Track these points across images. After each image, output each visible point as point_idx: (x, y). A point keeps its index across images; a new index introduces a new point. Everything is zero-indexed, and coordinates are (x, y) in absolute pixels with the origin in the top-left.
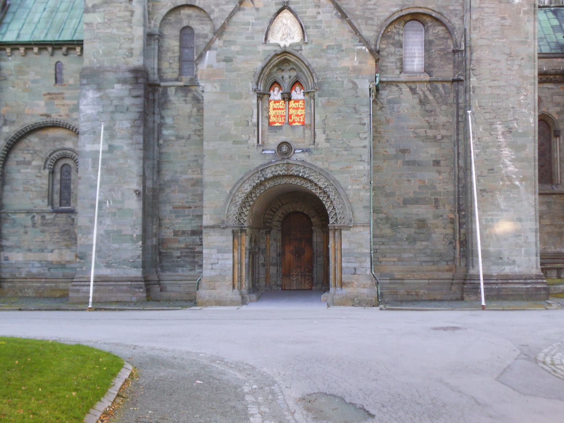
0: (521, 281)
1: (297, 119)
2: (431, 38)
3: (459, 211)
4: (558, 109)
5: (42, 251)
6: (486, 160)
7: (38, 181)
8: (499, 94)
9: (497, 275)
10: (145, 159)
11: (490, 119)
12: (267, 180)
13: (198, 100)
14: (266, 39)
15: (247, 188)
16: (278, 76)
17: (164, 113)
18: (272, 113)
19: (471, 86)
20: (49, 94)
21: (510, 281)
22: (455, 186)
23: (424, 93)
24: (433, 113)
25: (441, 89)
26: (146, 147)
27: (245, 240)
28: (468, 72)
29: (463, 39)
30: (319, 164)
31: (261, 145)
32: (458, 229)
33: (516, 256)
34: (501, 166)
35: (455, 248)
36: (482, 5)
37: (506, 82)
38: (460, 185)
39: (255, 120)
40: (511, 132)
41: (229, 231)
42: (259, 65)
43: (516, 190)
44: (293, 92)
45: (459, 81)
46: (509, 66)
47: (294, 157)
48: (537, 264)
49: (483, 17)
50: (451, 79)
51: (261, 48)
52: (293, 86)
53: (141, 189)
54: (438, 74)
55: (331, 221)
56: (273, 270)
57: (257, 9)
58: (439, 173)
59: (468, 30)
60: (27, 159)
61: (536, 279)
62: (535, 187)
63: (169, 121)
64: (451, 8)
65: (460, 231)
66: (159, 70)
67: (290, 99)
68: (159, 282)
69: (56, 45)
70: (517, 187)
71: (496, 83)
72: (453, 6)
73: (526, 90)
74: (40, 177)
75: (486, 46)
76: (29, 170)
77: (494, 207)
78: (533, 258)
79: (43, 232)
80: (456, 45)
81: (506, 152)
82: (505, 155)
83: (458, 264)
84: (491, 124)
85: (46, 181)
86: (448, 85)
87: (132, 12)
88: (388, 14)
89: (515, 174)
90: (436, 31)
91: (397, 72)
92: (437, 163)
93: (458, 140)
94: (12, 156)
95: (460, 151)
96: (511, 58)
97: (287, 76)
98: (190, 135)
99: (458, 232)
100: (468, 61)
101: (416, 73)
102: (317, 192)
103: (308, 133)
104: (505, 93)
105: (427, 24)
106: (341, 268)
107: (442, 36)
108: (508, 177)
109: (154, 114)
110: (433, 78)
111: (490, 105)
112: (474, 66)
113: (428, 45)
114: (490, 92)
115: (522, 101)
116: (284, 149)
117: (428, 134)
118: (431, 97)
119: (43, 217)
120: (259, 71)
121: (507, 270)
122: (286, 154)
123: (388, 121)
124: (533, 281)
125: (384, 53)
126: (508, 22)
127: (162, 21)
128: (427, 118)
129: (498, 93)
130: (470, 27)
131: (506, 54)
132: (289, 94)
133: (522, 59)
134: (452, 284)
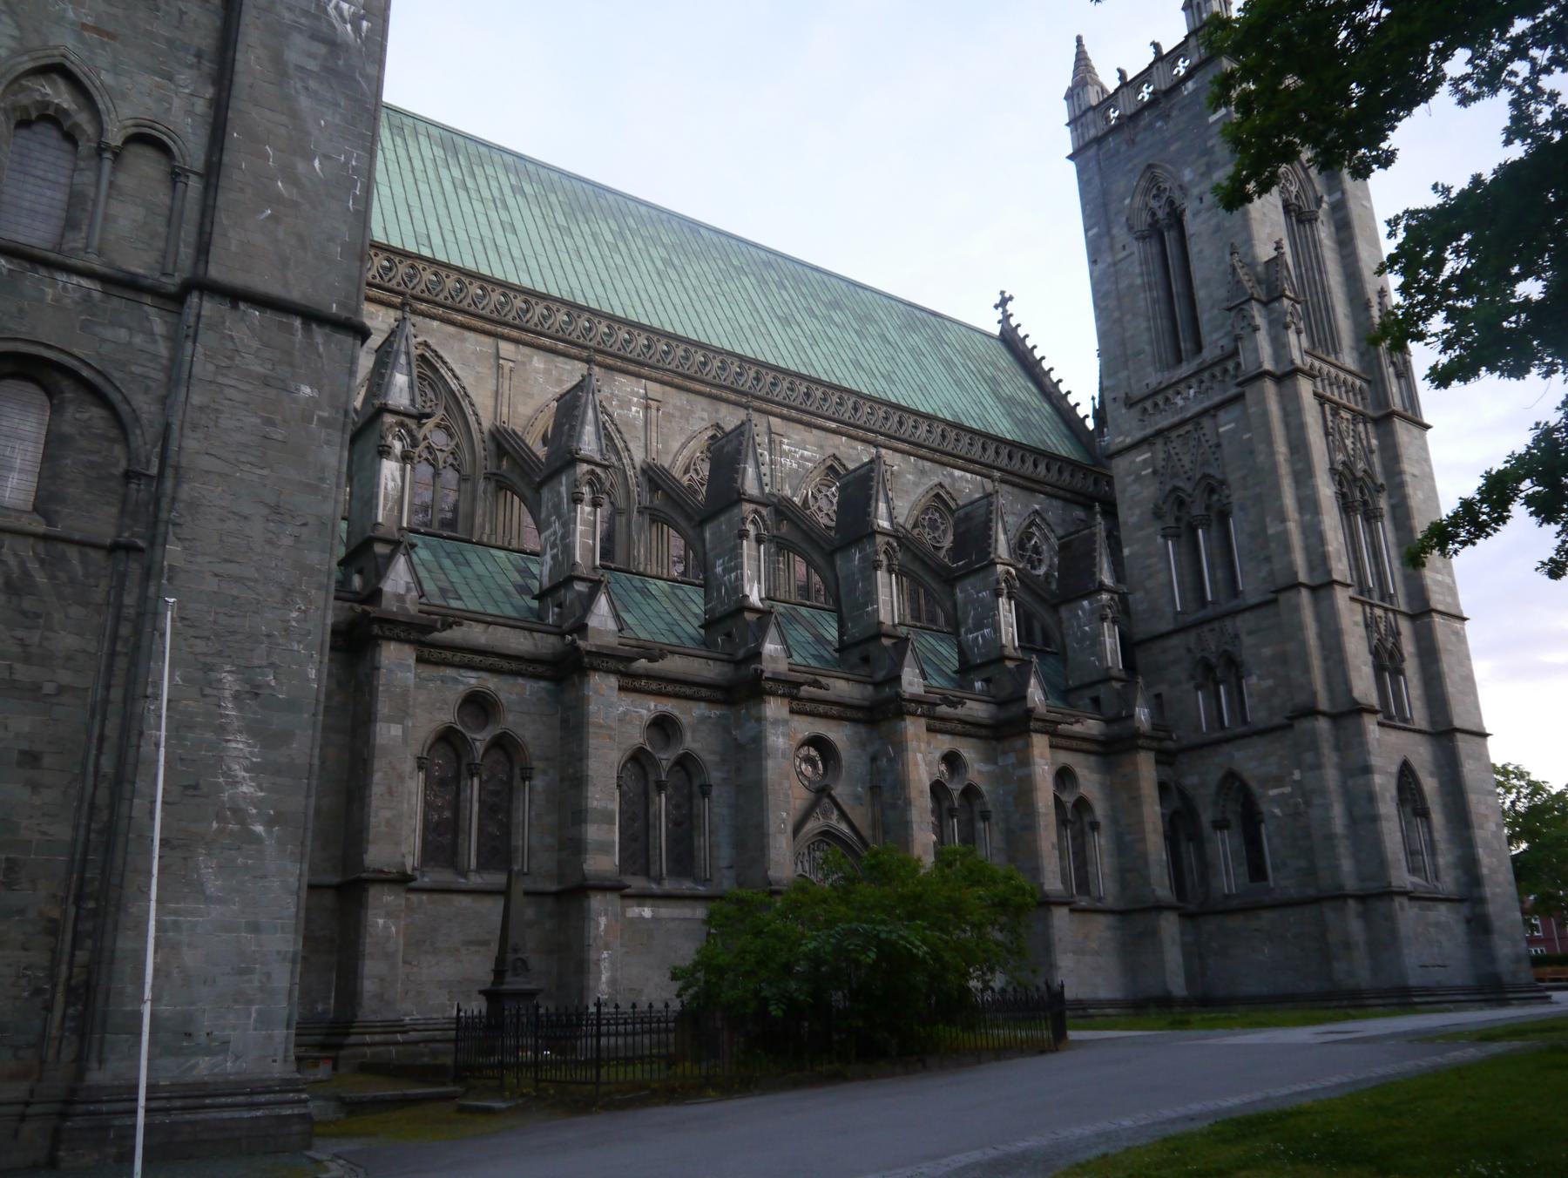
0: (241, 1099)
2: (66, 429)
3: (79, 898)
6: (182, 759)
8: (237, 598)
9: (172, 1085)
11: (205, 655)
19: (165, 563)
21: (208, 1101)
22: (76, 828)
23: (22, 564)
24: (41, 621)
25: (75, 562)
28: (161, 528)
29: (157, 450)
32: (67, 948)
33: (234, 1028)
34: (221, 780)
35: (48, 1008)
36: (220, 380)
37: (257, 570)
38: (93, 826)
40: (257, 694)
43: (254, 847)
45: (130, 548)
46: (270, 535)
48: (286, 1050)
49: (220, 408)
50: (108, 541)
54: (71, 522)
58: (35, 787)
59: (176, 428)
61: (280, 1092)
62: (302, 843)
65: (72, 955)
70: (256, 839)
71: (232, 569)
72: (143, 366)
73: (305, 595)
75: (220, 474)
77: (186, 890)
81: (239, 745)
82: (235, 753)
83: (51, 1053)
84: (208, 668)
89: (257, 803)
90: (86, 416)
92: (31, 758)
93: (106, 701)
95: (108, 731)
96: (277, 517)
99: (66, 958)
100: (165, 503)
101: (7, 508)
104: (254, 596)
105: (62, 392)
107: (99, 431)
108: (236, 811)
110: (58, 530)
111: (211, 619)
112: (181, 516)
113: (54, 445)
114: (216, 589)
115: (294, 624)
117: (16, 677)
118: (41, 579)
124: (271, 1097)
126: (279, 434)
128: (20, 633)
129: (235, 592)
130: (183, 422)
131: (267, 505)
133: (305, 525)
134: (23, 1118)
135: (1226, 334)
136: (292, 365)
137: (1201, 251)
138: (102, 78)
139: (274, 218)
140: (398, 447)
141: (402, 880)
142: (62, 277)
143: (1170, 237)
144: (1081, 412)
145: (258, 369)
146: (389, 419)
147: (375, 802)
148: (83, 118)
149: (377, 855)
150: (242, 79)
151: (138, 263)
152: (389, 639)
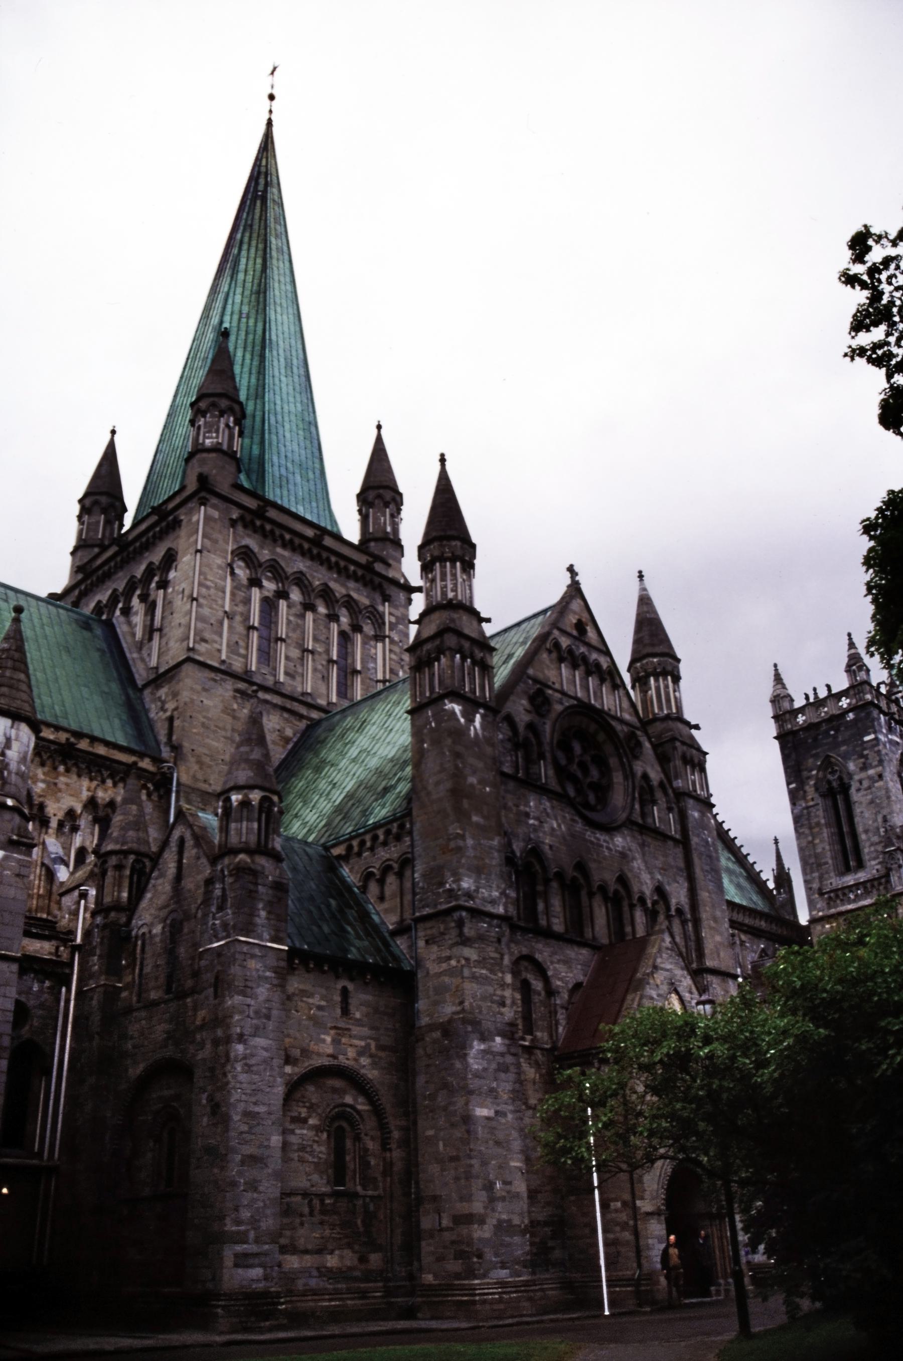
7: (315, 1146)
20: (335, 1028)
60: (303, 1115)
74: (317, 1142)
76: (305, 1132)
79: (322, 1223)
119: (322, 1202)
135: (880, 863)
137: (862, 812)
143: (839, 798)
144: (764, 876)
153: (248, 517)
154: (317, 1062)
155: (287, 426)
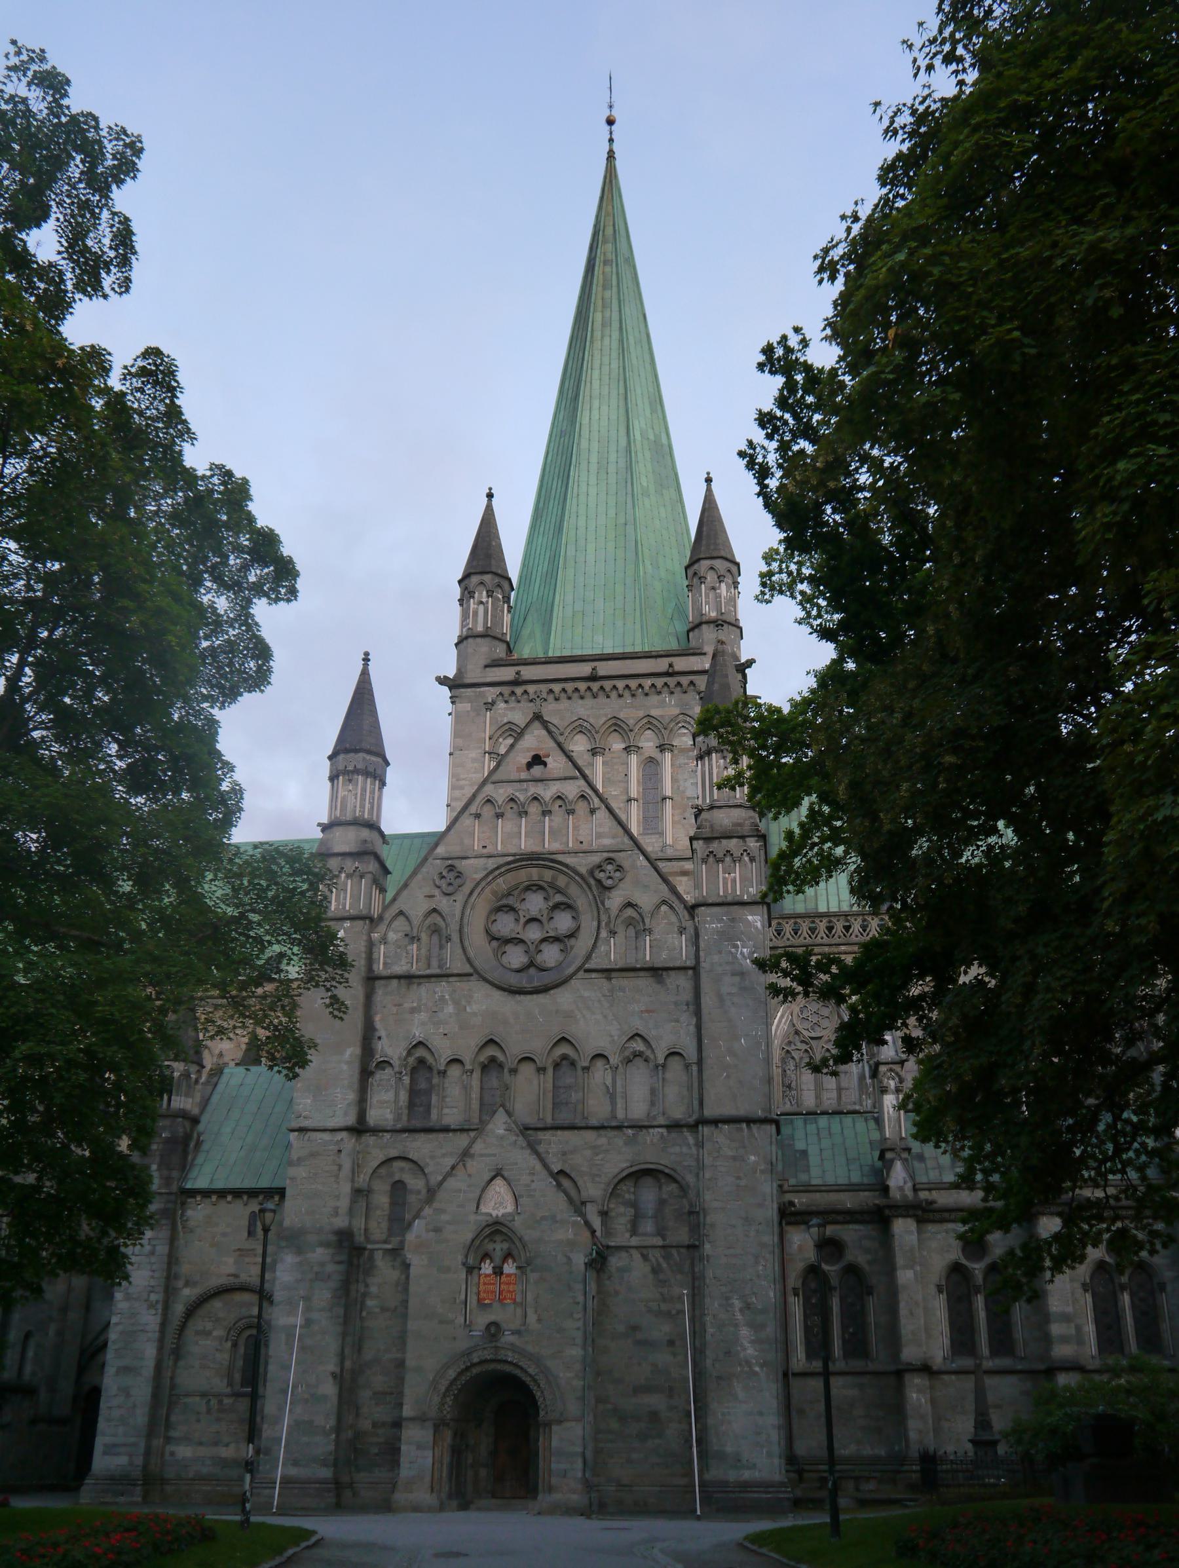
1: (509, 1295)
2: (665, 1196)
4: (869, 1257)
5: (216, 1444)
10: (344, 1335)
12: (474, 1365)
13: (406, 1266)
14: (478, 1207)
15: (452, 1374)
16: (490, 1246)
17: (370, 1280)
18: (482, 1288)
26: (346, 1321)
27: (448, 1435)
30: (530, 1348)
31: (468, 1326)
39: (463, 1297)
41: (429, 1424)
42: (470, 1236)
44: (506, 1265)
47: (503, 1340)
51: (472, 1218)
52: (504, 1260)
53: (338, 1370)
55: (542, 1413)
56: (483, 1472)
57: (470, 1176)
58: (674, 1355)
63: (374, 1289)
64: (686, 1164)
66: (366, 1230)
67: (502, 1273)
68: (351, 1485)
69: (253, 1193)
70: (756, 1374)
76: (209, 1342)
78: (776, 1461)
79: (218, 1420)
80: (691, 1205)
81: (744, 1332)
84: (727, 1299)
85: (226, 1356)
86: (683, 1251)
87: (340, 1167)
88: (616, 1171)
91: (627, 1235)
92: (671, 1343)
94: (190, 1324)
97: (498, 1248)
98: (396, 1307)
102: (527, 1379)
103: (519, 1311)
106: (550, 1470)
109: (357, 1281)
110: (667, 1242)
116: (493, 1330)
118: (665, 1265)
119: (220, 1402)
120: (468, 1242)
121: (747, 1475)
122: (493, 1336)
123: (617, 1293)
125: (613, 1214)
127: (374, 1171)
132: (501, 1268)
136: (744, 1147)
138: (650, 1034)
139: (728, 1077)
140: (892, 1084)
141: (925, 1369)
142: (651, 1130)
145: (730, 1154)
146: (883, 1069)
147: (903, 1321)
148: (648, 1053)
149: (910, 1354)
150: (705, 1011)
151: (678, 1113)
152: (897, 1216)
153: (506, 690)
154: (214, 1282)
155: (591, 548)
